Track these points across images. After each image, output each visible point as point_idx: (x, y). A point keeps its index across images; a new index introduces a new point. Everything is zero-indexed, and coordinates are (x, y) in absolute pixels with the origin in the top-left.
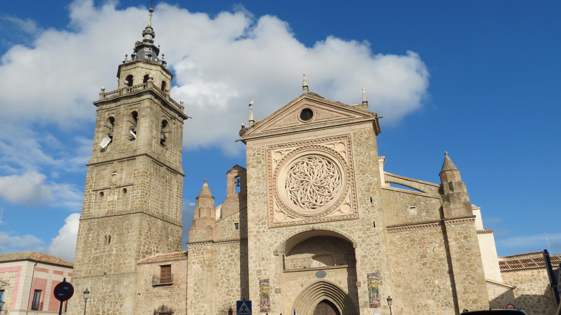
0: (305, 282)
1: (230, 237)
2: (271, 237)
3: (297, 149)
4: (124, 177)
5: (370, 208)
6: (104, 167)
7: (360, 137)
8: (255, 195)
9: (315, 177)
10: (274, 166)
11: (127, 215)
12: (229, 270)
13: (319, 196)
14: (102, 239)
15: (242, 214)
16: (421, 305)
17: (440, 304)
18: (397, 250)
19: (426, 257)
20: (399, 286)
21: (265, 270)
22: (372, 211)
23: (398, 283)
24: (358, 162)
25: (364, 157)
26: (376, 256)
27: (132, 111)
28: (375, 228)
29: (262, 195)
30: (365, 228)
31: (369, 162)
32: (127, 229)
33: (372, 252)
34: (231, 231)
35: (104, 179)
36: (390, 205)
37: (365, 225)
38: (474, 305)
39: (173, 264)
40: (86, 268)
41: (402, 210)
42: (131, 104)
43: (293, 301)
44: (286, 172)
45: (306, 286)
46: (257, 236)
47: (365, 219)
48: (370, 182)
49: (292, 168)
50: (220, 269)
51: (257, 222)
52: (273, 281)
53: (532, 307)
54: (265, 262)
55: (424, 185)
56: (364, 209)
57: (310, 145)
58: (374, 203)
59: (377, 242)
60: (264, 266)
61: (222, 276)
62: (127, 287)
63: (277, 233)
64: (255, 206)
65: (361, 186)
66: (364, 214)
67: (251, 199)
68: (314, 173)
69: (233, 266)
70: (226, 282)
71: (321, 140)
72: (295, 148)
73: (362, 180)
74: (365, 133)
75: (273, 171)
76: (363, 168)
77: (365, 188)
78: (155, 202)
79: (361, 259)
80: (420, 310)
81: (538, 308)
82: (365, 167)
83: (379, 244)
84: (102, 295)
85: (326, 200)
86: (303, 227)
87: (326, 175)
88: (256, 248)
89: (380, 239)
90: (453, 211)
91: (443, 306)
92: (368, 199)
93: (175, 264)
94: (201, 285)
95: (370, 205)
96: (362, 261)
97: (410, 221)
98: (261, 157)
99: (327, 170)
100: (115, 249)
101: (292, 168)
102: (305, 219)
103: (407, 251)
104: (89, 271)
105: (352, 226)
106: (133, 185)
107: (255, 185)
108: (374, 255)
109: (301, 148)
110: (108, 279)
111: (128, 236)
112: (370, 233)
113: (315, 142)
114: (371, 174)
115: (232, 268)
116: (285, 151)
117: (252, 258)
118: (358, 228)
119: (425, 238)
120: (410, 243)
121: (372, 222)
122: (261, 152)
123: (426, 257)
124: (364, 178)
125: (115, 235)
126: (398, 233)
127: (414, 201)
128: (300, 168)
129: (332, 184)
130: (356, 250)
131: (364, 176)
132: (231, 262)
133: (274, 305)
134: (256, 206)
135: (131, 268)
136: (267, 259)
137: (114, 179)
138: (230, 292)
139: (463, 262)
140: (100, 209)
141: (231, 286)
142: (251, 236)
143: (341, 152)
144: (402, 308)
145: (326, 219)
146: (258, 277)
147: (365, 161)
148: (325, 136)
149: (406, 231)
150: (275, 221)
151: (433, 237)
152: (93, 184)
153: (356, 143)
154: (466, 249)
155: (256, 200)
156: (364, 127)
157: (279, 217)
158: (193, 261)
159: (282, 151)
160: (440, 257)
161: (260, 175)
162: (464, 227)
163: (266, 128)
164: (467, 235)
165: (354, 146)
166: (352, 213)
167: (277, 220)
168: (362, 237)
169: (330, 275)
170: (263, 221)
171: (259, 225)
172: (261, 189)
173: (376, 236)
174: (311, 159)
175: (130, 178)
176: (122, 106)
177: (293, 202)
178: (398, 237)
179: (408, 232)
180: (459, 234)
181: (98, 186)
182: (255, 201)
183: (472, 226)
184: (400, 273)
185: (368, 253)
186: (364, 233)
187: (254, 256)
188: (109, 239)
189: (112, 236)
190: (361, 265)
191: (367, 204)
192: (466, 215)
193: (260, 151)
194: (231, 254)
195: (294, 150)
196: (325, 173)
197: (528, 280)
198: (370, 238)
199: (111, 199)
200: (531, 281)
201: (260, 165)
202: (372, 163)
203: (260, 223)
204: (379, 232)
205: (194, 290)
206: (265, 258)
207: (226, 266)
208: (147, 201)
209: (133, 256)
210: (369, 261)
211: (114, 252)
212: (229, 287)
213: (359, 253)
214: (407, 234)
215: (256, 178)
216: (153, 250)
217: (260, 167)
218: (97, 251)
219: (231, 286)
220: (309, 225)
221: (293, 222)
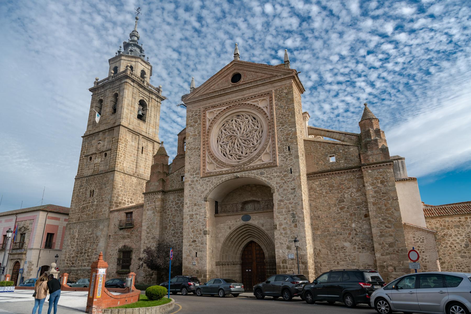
0: (233, 225)
3: (227, 108)
4: (106, 144)
8: (192, 150)
10: (208, 124)
12: (175, 215)
13: (244, 148)
14: (88, 193)
16: (338, 247)
17: (357, 247)
18: (316, 196)
19: (344, 201)
20: (318, 229)
21: (197, 214)
23: (317, 227)
26: (292, 201)
28: (291, 175)
29: (197, 150)
31: (288, 115)
32: (105, 184)
35: (93, 146)
36: (310, 154)
37: (283, 171)
38: (390, 248)
39: (134, 211)
41: (322, 158)
43: (222, 242)
45: (233, 228)
46: (192, 184)
49: (224, 125)
50: (168, 215)
53: (459, 252)
55: (344, 135)
56: (282, 157)
57: (237, 104)
58: (292, 151)
59: (293, 187)
61: (170, 220)
62: (102, 230)
63: (208, 181)
65: (281, 137)
66: (282, 162)
67: (188, 153)
68: (241, 128)
69: (178, 212)
70: (173, 226)
71: (247, 98)
72: (225, 108)
73: (281, 131)
74: (286, 88)
75: (207, 129)
76: (282, 120)
77: (284, 138)
78: (130, 163)
79: (278, 203)
80: (337, 252)
81: (465, 253)
83: (295, 189)
85: (250, 151)
87: (251, 129)
90: (370, 157)
91: (360, 248)
92: (286, 148)
93: (136, 211)
94: (152, 228)
95: (287, 154)
96: (279, 205)
97: (329, 168)
99: (252, 125)
100: (96, 200)
101: (224, 125)
103: (326, 197)
106: (111, 150)
107: (192, 141)
108: (290, 200)
109: (230, 107)
111: (105, 190)
114: (290, 125)
116: (216, 111)
117: (186, 204)
119: (343, 184)
121: (289, 168)
122: (198, 113)
123: (344, 201)
126: (317, 180)
127: (334, 150)
128: (230, 124)
129: (255, 137)
130: (274, 194)
131: (283, 127)
132: (177, 209)
133: (202, 245)
134: (192, 159)
136: (199, 205)
137: (99, 146)
139: (379, 206)
140: (89, 169)
143: (264, 107)
144: (320, 250)
145: (249, 168)
146: (190, 220)
147: (285, 113)
148: (251, 95)
149: (325, 178)
150: (207, 171)
151: (351, 183)
154: (383, 193)
155: (192, 154)
156: (285, 83)
157: (209, 168)
158: (148, 208)
159: (215, 111)
160: (358, 201)
161: (196, 133)
162: (381, 172)
163: (203, 93)
164: (384, 179)
166: (271, 161)
167: (208, 170)
168: (280, 183)
169: (254, 219)
171: (193, 175)
173: (293, 181)
174: (239, 116)
175: (110, 144)
176: (108, 90)
177: (222, 155)
178: (317, 183)
179: (327, 179)
180: (376, 179)
181: (89, 152)
182: (191, 155)
183: (389, 170)
184: (319, 217)
185: (284, 197)
187: (188, 202)
188: (92, 193)
189: (95, 190)
190: (277, 209)
191: (285, 153)
192: (384, 160)
193: (197, 112)
194: (177, 201)
195: (225, 110)
196: (250, 127)
197: (455, 226)
198: (287, 184)
199: (96, 162)
200: (458, 227)
201: (196, 124)
203: (194, 173)
204: (295, 177)
205: (147, 232)
207: (173, 212)
208: (122, 162)
209: (108, 205)
210: (285, 205)
211: (95, 203)
213: (276, 197)
214: (326, 180)
216: (127, 201)
217: (197, 125)
218: (84, 202)
221: (221, 171)
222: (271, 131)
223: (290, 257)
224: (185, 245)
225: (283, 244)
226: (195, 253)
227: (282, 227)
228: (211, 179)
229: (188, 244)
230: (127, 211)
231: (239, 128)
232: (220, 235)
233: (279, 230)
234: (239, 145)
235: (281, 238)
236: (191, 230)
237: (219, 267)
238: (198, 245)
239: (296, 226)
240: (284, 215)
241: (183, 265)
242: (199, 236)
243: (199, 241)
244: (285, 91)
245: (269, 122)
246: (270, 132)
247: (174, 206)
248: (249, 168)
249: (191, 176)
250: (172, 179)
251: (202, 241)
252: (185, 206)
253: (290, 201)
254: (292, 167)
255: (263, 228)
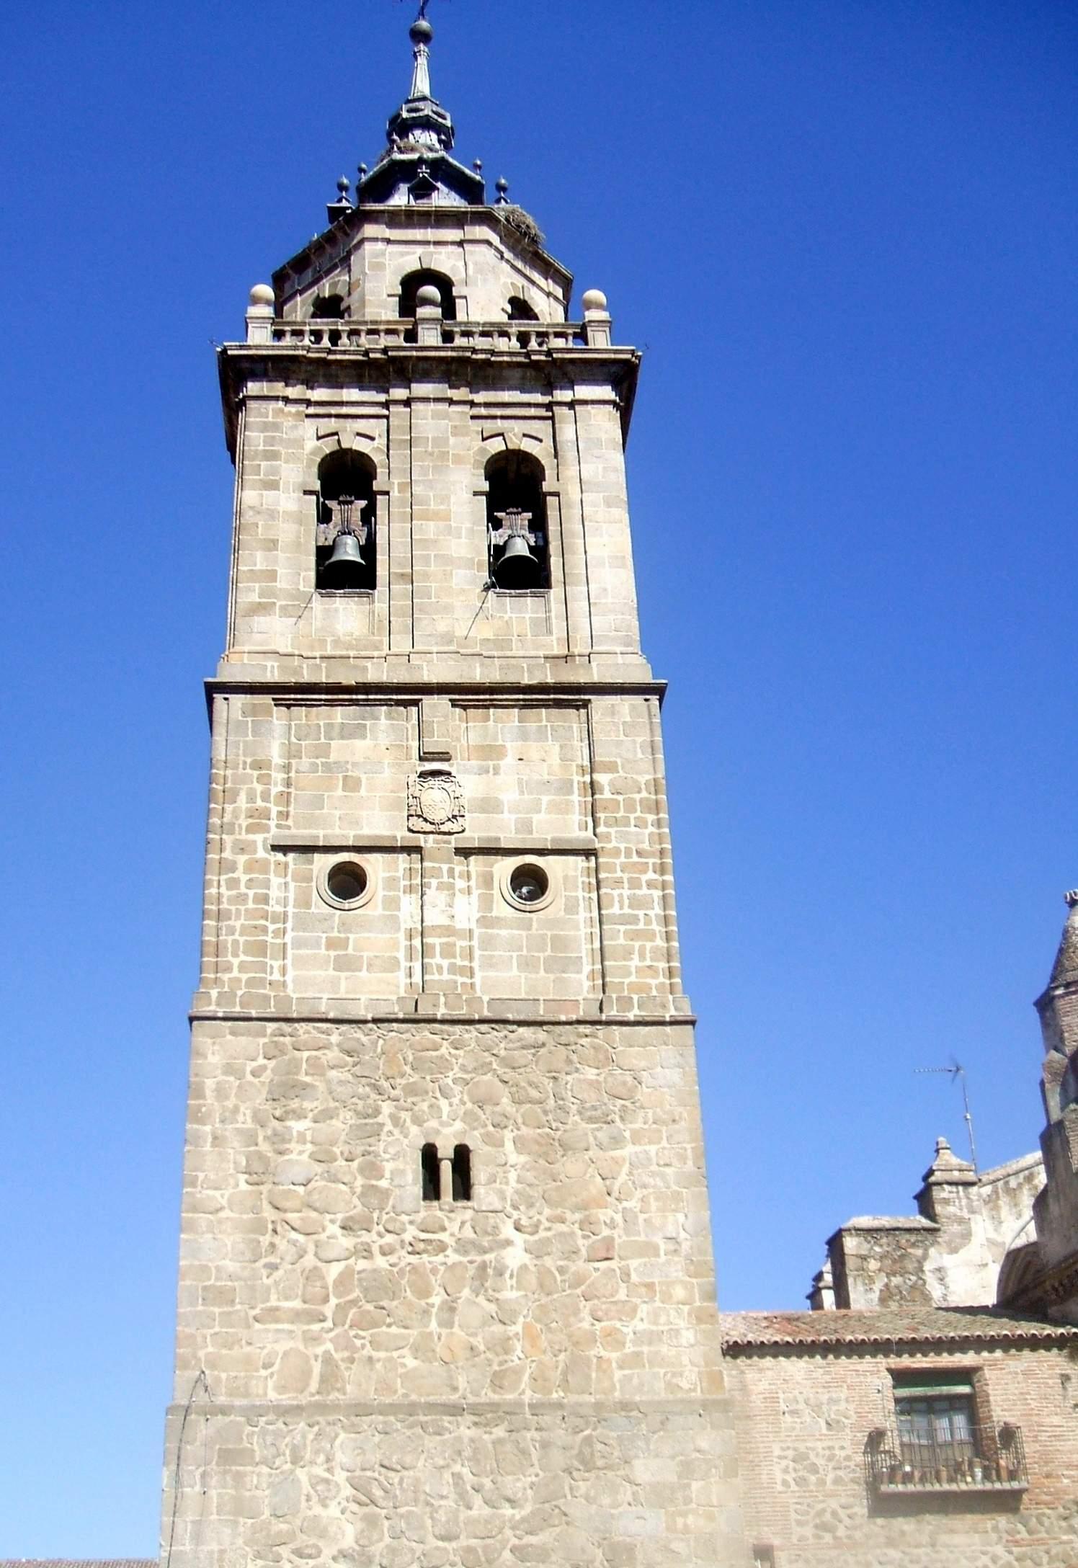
6: (339, 715)
11: (583, 1029)
27: (497, 446)
40: (282, 1347)
42: (483, 411)
84: (464, 1541)
100: (518, 1238)
104: (317, 1368)
110: (500, 1432)
125: (509, 1145)
135: (674, 1375)
152: (274, 810)
181: (311, 822)
211: (515, 1257)
218: (365, 1237)
230: (906, 1362)
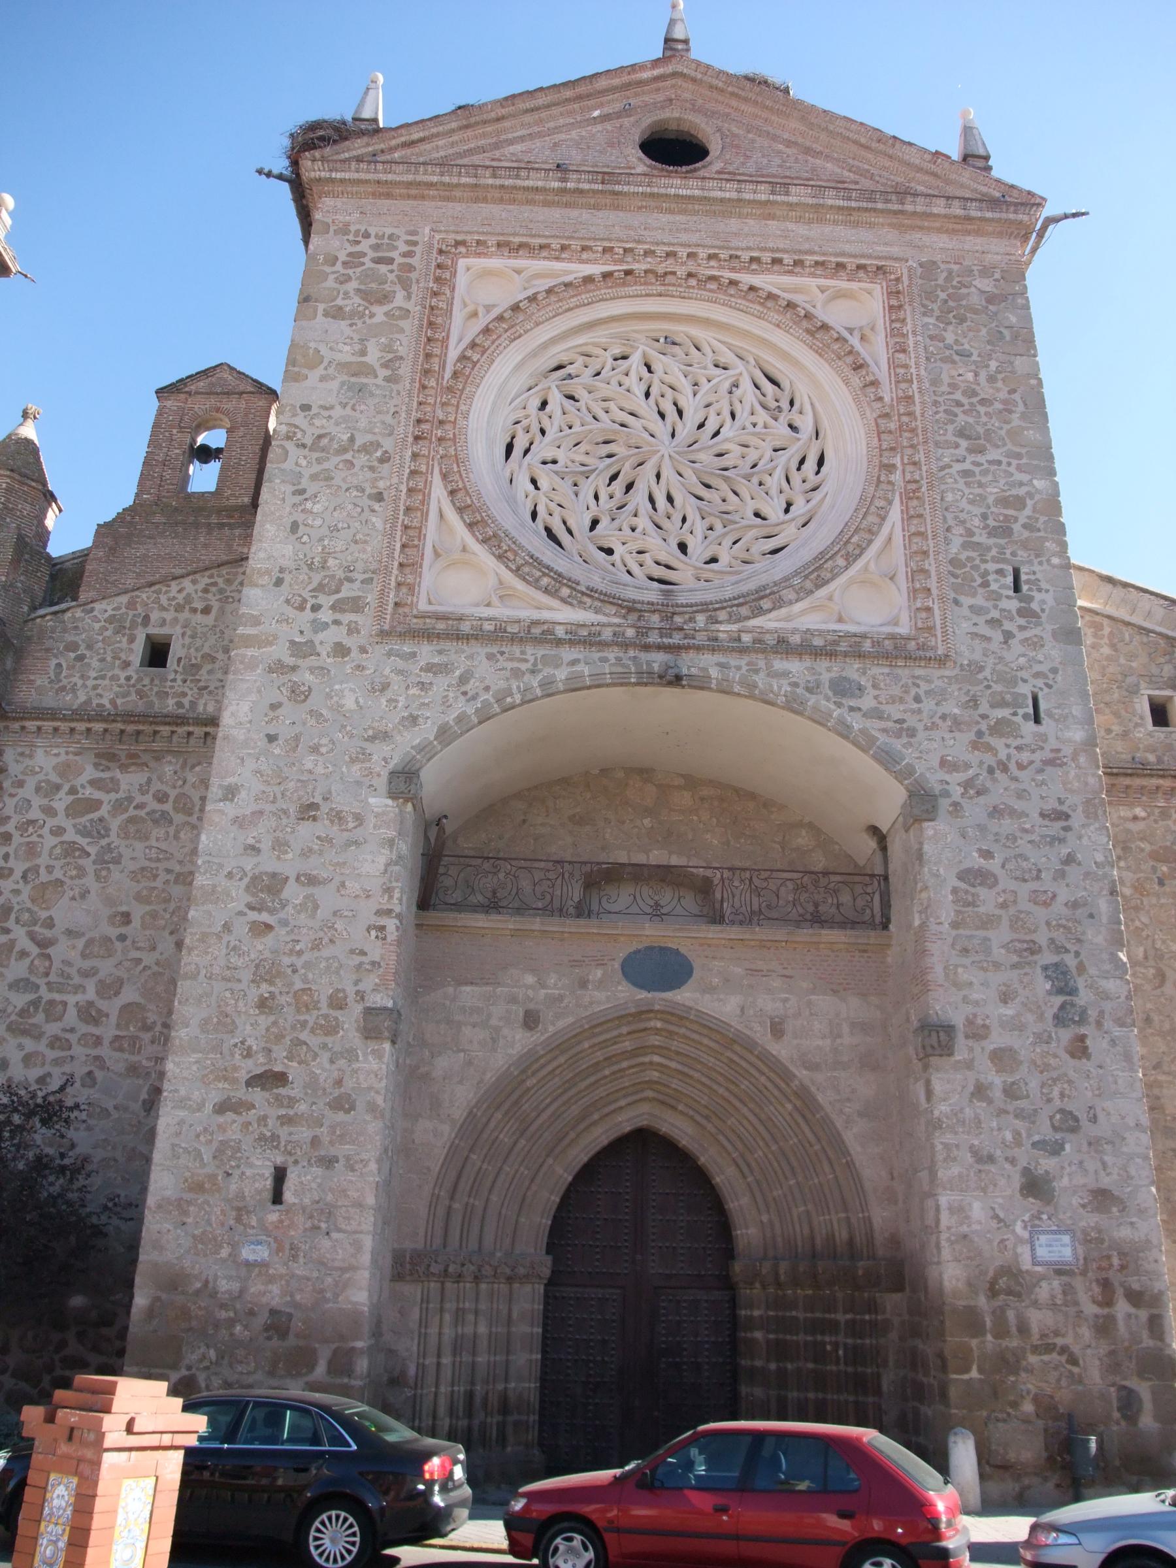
1: (105, 702)
2: (385, 687)
3: (606, 276)
5: (1012, 620)
7: (954, 283)
9: (686, 429)
15: (206, 591)
22: (1027, 634)
24: (945, 388)
25: (976, 375)
28: (1041, 729)
30: (984, 717)
31: (1005, 402)
33: (1027, 859)
34: (117, 671)
44: (523, 380)
45: (555, 1025)
46: (294, 668)
47: (987, 673)
48: (1014, 492)
51: (306, 594)
52: (358, 959)
54: (322, 828)
56: (976, 619)
59: (1051, 804)
60: (306, 853)
63: (429, 668)
64: (309, 505)
65: (964, 504)
67: (289, 465)
69: (87, 863)
70: (23, 954)
71: (746, 256)
73: (966, 473)
75: (453, 354)
77: (984, 517)
79: (955, 891)
82: (984, 419)
86: (604, 660)
88: (271, 738)
89: (1072, 791)
92: (1000, 572)
96: (965, 902)
98: (391, 277)
102: (616, 620)
105: (909, 698)
107: (332, 400)
108: (1038, 878)
109: (628, 273)
112: (1012, 751)
113: (713, 263)
114: (1018, 456)
115: (82, 872)
117: (230, 793)
118: (941, 710)
120: (1154, 869)
121: (1025, 689)
122: (394, 254)
124: (977, 470)
129: (779, 474)
132: (83, 841)
133: (341, 1116)
134: (317, 508)
136: (338, 817)
138: (40, 1018)
141: (53, 978)
142: (252, 666)
143: (851, 331)
145: (746, 638)
146: (253, 916)
153: (935, 307)
159: (518, 272)
165: (924, 314)
166: (904, 629)
168: (967, 766)
170: (346, 591)
171: (316, 608)
172: (363, 424)
173: (1049, 769)
182: (314, 477)
186: (975, 746)
190: (955, 925)
193: (396, 248)
195: (588, 280)
201: (380, 311)
202: (1021, 408)
203: (326, 601)
204: (1067, 751)
206: (325, 808)
207: (43, 860)
212: (41, 982)
215: (343, 366)
217: (380, 318)
219: (53, 978)
220: (644, 656)
222: (897, 461)
223: (1042, 1253)
224: (182, 1103)
225: (991, 1159)
226: (268, 1172)
227: (990, 1045)
228: (461, 657)
229: (215, 1097)
231: (670, 411)
232: (442, 1064)
233: (969, 1065)
234: (661, 501)
235: (978, 1122)
236: (254, 994)
237: (412, 1291)
238: (302, 1107)
239: (1079, 1049)
240: (997, 965)
241: (146, 1256)
242: (314, 1041)
243: (312, 1085)
244: (986, 285)
245: (887, 415)
246: (891, 468)
247: (61, 820)
248: (746, 638)
249: (291, 612)
250: (69, 638)
251: (339, 1083)
252: (219, 812)
253: (1033, 885)
254: (1040, 683)
255: (781, 1050)
